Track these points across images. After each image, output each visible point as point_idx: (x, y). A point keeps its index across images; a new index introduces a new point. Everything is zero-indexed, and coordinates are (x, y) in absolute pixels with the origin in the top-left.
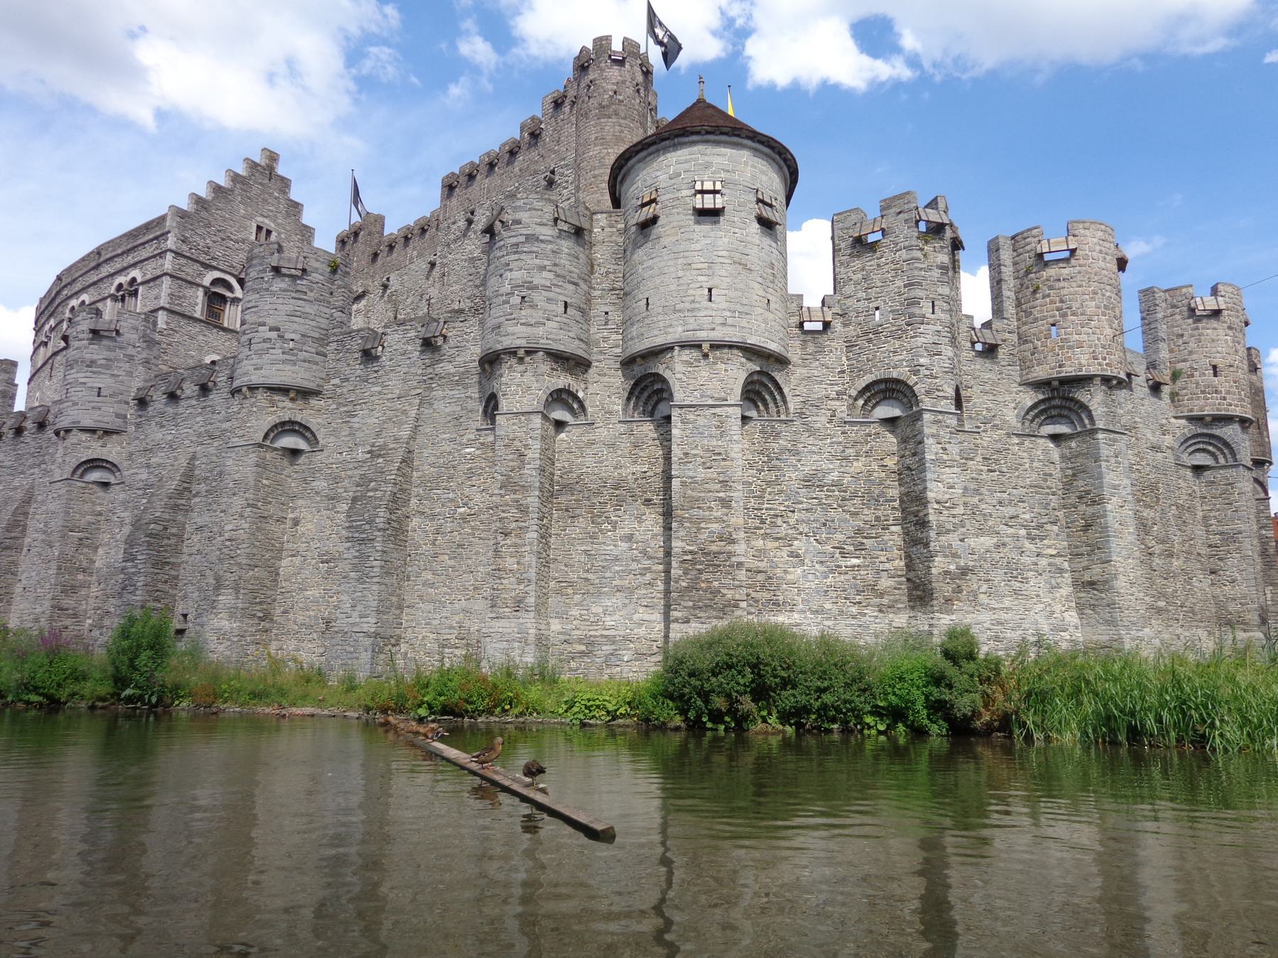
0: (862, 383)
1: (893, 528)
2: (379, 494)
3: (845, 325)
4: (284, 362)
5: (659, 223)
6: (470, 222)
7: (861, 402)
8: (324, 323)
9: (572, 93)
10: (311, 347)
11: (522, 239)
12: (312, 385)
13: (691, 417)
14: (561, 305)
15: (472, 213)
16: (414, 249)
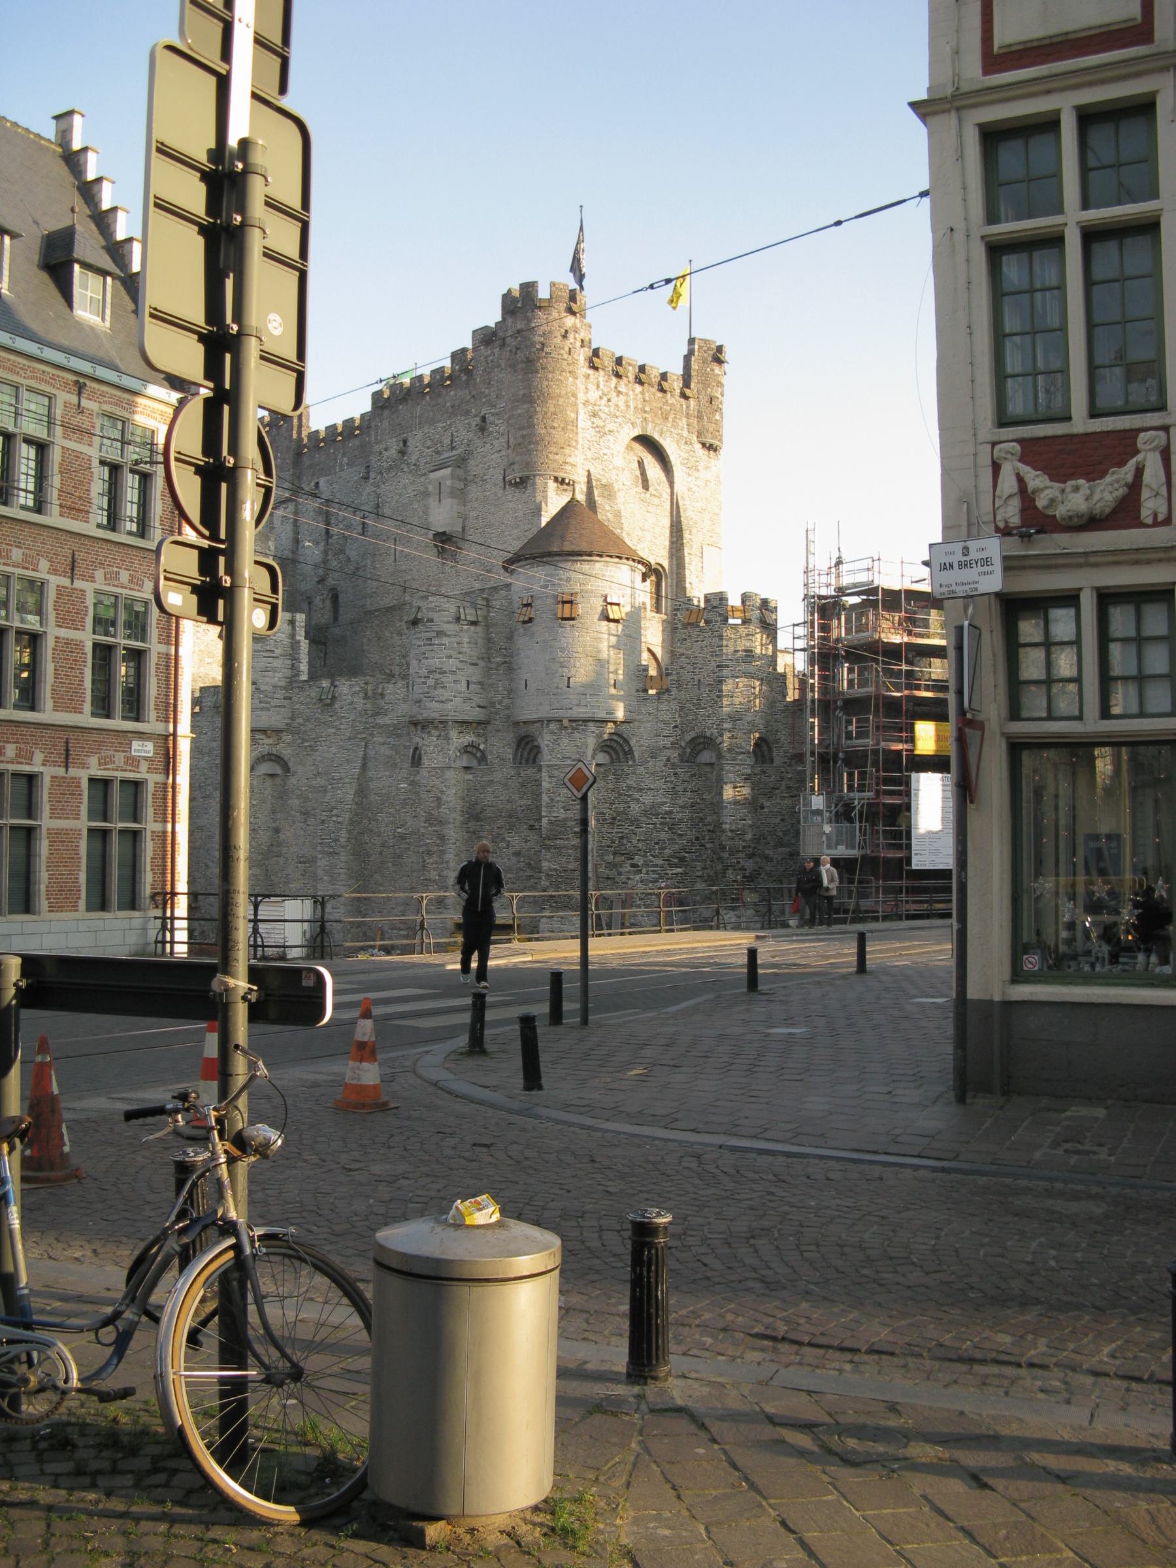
0: (688, 738)
1: (708, 845)
2: (340, 820)
3: (680, 691)
4: (262, 709)
5: (535, 621)
6: (402, 453)
7: (688, 750)
8: (288, 673)
9: (501, 334)
10: (280, 694)
11: (434, 634)
12: (282, 726)
13: (556, 773)
14: (464, 684)
15: (405, 442)
16: (344, 455)
